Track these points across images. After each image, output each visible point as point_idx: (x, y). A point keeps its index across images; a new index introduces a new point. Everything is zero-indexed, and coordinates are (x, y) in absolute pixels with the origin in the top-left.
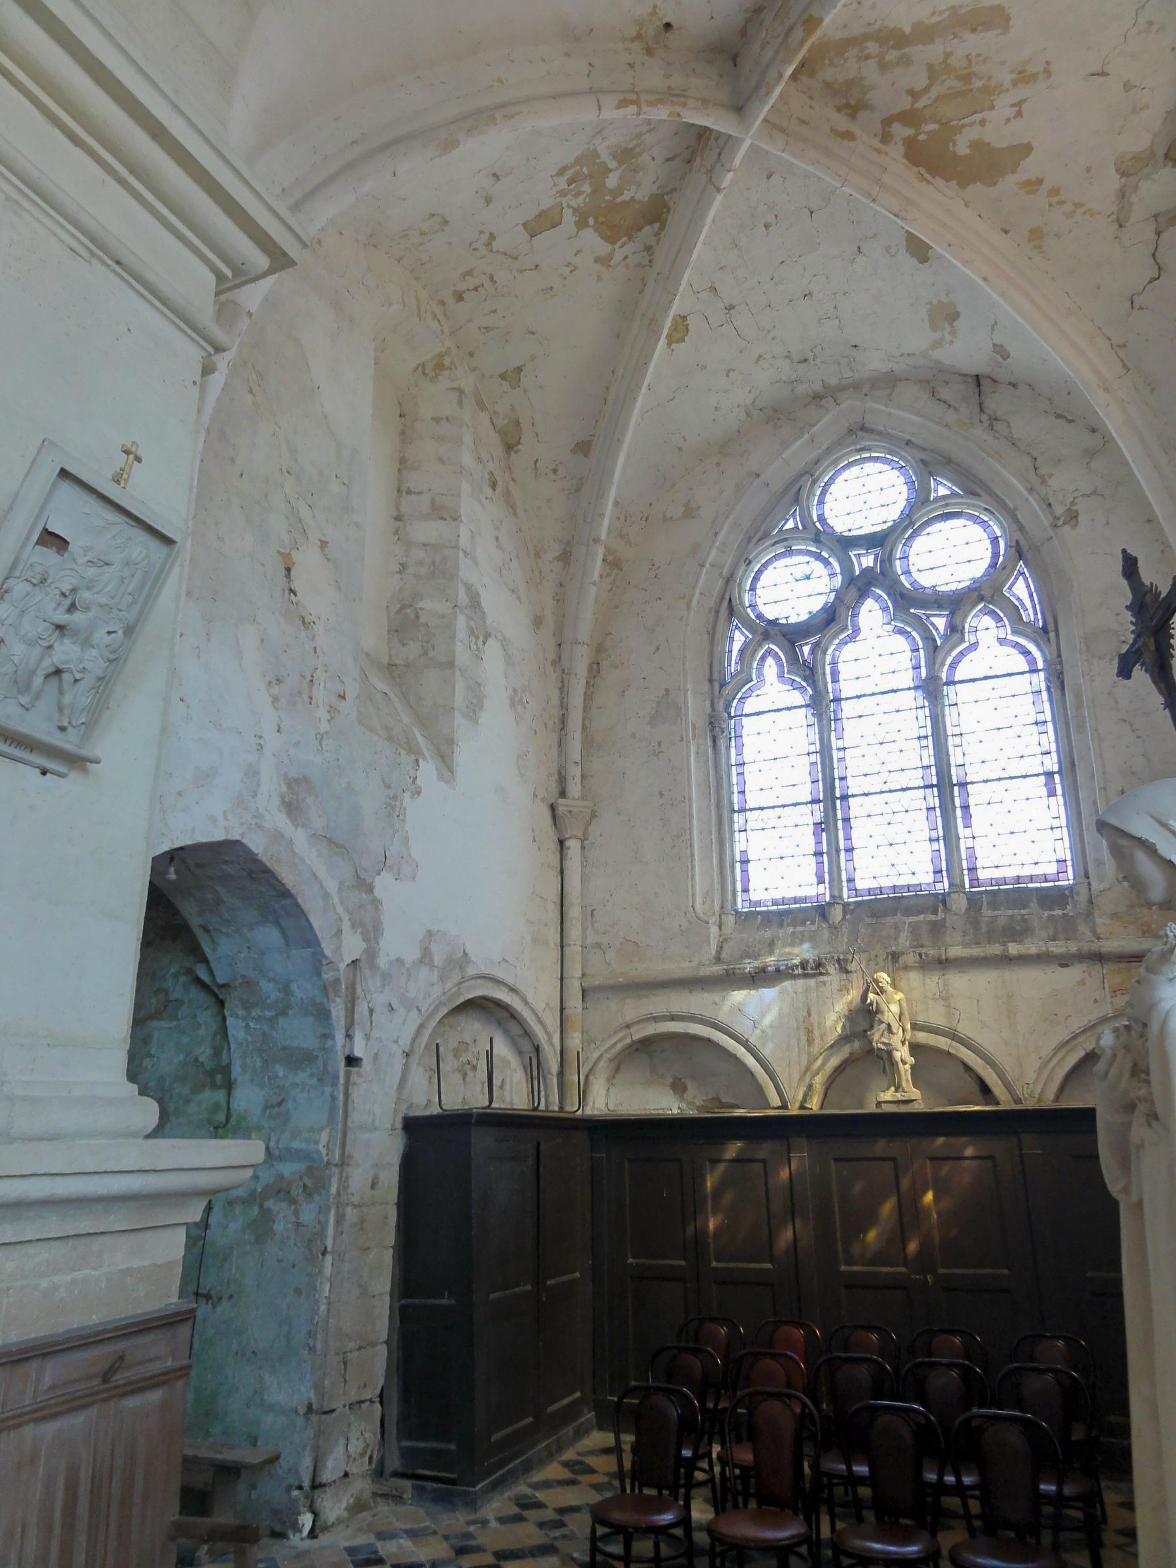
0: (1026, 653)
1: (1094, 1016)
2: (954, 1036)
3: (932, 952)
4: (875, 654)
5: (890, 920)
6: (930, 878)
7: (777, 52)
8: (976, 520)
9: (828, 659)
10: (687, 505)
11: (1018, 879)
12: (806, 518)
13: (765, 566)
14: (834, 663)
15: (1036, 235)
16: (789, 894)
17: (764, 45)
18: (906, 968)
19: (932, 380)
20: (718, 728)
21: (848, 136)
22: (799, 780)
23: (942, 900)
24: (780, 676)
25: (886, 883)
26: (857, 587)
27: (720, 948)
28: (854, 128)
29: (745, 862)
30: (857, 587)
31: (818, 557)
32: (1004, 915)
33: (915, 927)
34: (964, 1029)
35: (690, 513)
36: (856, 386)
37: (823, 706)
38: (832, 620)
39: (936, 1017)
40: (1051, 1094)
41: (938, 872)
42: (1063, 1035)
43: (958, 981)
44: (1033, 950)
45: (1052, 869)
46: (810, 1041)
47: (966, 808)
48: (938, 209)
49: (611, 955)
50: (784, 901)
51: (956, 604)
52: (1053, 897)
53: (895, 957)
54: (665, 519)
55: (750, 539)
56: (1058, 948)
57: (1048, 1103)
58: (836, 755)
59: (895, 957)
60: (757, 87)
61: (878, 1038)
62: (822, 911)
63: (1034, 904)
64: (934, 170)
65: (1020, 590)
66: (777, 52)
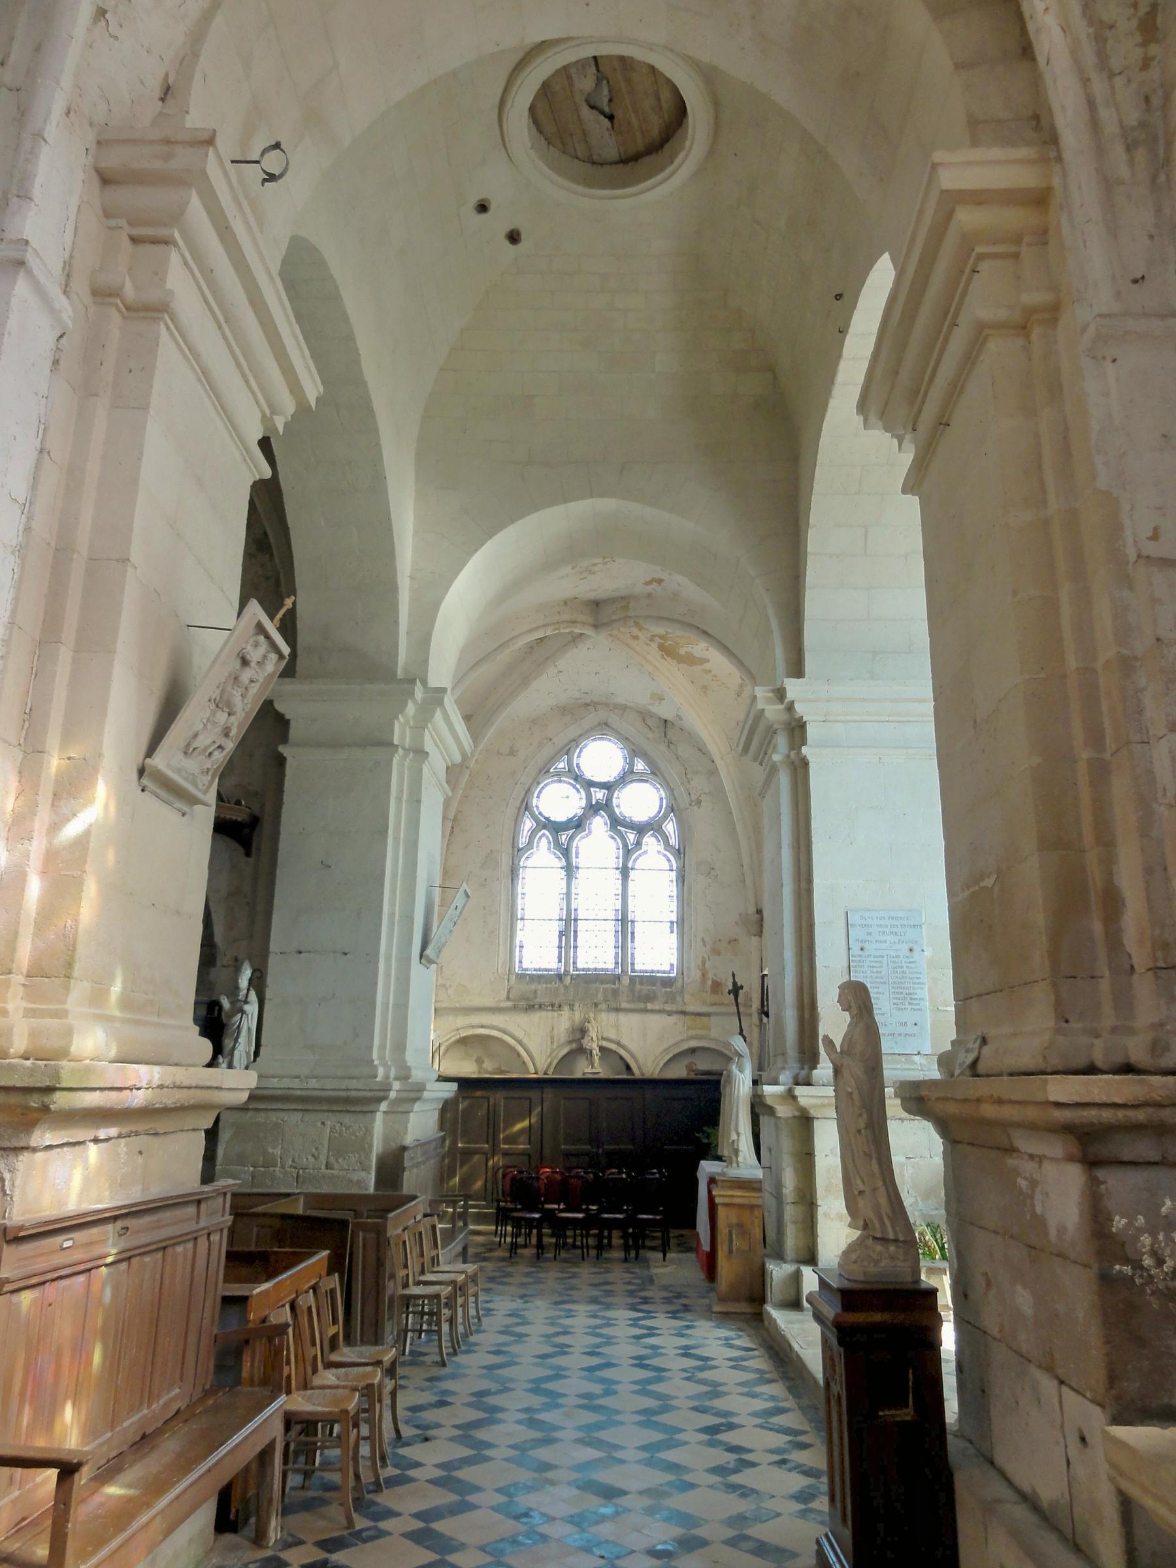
0: (669, 861)
1: (679, 1038)
2: (619, 1044)
3: (614, 1005)
4: (597, 846)
5: (594, 986)
6: (612, 966)
7: (619, 620)
8: (654, 786)
9: (575, 844)
10: (511, 748)
11: (652, 972)
12: (570, 763)
13: (546, 785)
14: (577, 848)
15: (704, 688)
16: (543, 967)
17: (613, 613)
18: (601, 1010)
19: (644, 715)
20: (514, 873)
21: (636, 638)
22: (555, 908)
23: (618, 977)
24: (549, 849)
25: (592, 966)
26: (593, 809)
27: (509, 992)
28: (640, 635)
29: (521, 947)
30: (593, 809)
31: (574, 787)
32: (646, 988)
33: (605, 991)
34: (624, 1041)
35: (512, 752)
36: (607, 705)
37: (570, 870)
38: (578, 824)
39: (612, 1035)
40: (657, 1072)
41: (617, 963)
42: (666, 1045)
43: (624, 1018)
44: (657, 1008)
45: (668, 968)
46: (552, 1043)
47: (633, 933)
48: (669, 667)
49: (450, 991)
50: (540, 970)
51: (641, 829)
52: (667, 982)
53: (596, 1005)
54: (499, 753)
55: (540, 771)
56: (668, 1008)
57: (656, 1075)
58: (573, 896)
59: (596, 1005)
60: (606, 624)
61: (586, 1043)
62: (560, 977)
63: (658, 984)
64: (668, 655)
65: (670, 827)
66: (619, 620)
